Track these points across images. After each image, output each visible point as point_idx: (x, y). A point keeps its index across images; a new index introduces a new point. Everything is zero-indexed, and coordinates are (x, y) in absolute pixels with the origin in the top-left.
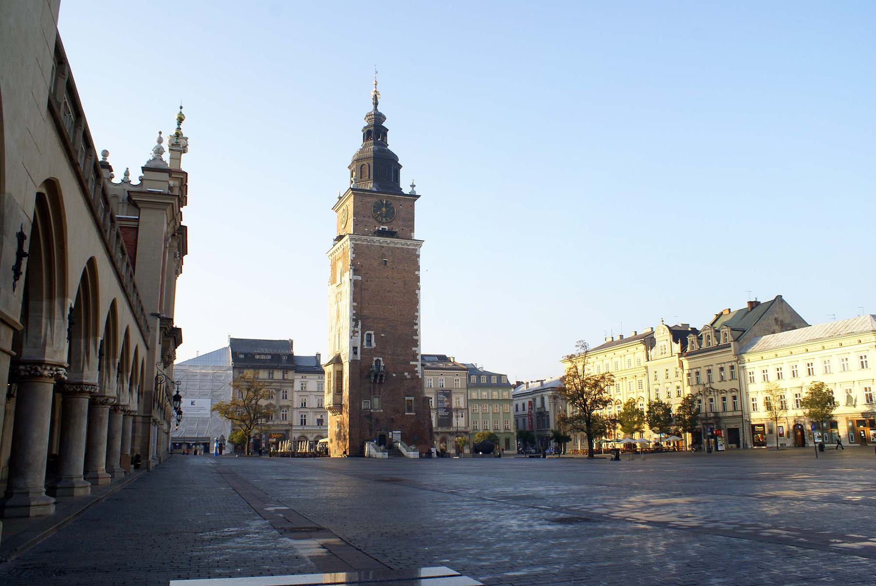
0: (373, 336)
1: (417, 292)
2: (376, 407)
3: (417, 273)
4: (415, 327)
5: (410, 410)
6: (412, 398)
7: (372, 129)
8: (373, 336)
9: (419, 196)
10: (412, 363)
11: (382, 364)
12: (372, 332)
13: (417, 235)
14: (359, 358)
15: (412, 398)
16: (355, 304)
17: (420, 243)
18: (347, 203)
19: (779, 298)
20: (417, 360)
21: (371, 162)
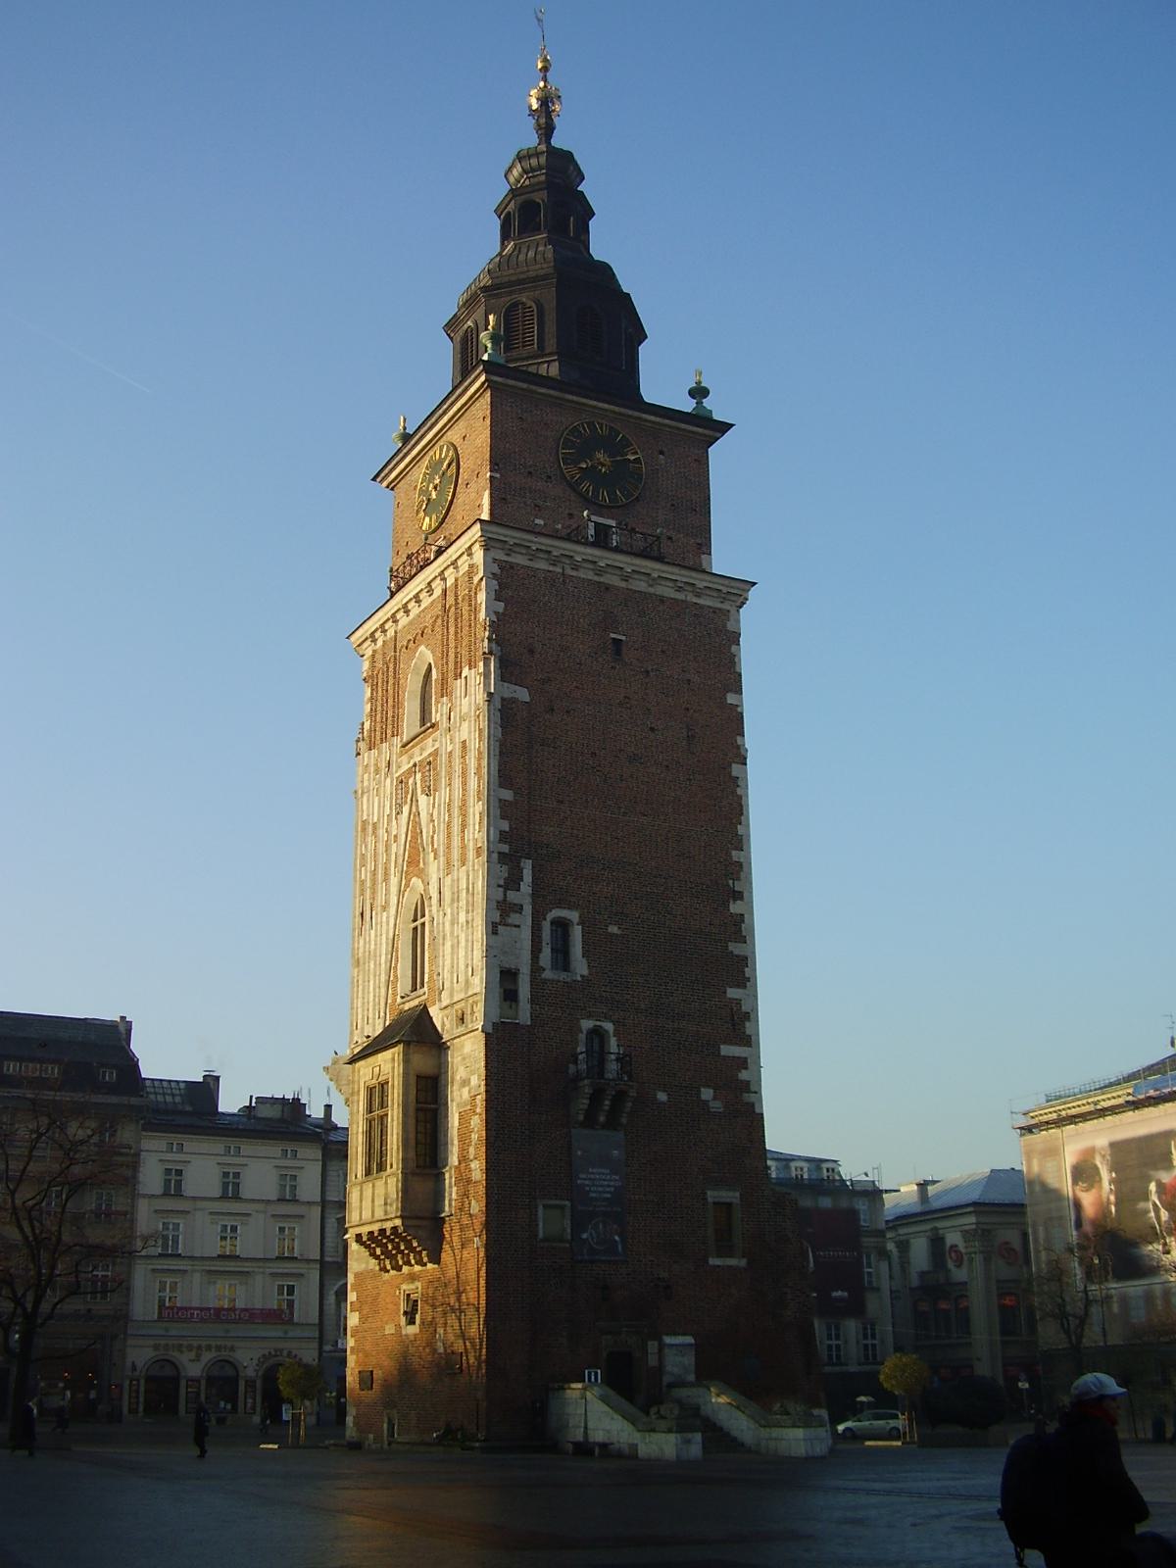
0: (577, 933)
3: (731, 699)
4: (735, 908)
6: (732, 1196)
7: (541, 197)
8: (577, 933)
9: (724, 427)
10: (727, 1050)
11: (613, 1044)
12: (574, 916)
13: (723, 560)
14: (524, 1014)
15: (732, 1196)
16: (507, 795)
17: (737, 591)
18: (454, 435)
21: (549, 296)
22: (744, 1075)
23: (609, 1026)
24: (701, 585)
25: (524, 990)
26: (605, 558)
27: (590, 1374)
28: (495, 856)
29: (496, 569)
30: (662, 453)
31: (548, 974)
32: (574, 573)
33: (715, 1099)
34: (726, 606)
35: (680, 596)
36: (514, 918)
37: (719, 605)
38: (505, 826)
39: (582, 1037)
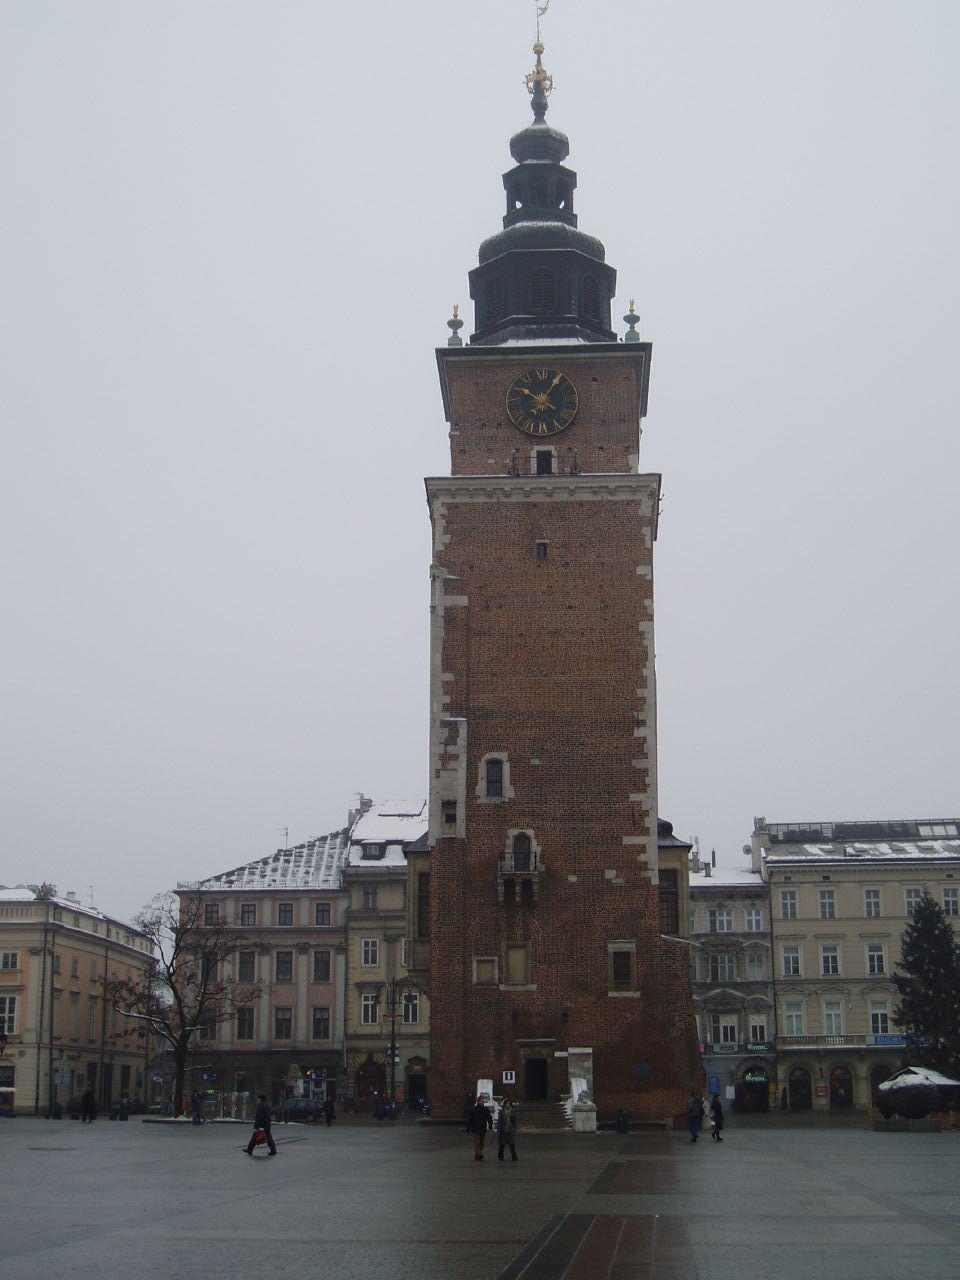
0: (506, 768)
1: (642, 626)
2: (518, 974)
4: (639, 733)
5: (622, 977)
6: (630, 946)
10: (627, 840)
12: (503, 756)
14: (460, 830)
16: (449, 677)
19: (650, 345)
20: (645, 832)
22: (643, 858)
23: (530, 832)
24: (612, 486)
25: (461, 812)
26: (528, 484)
27: (506, 1074)
28: (438, 723)
29: (444, 511)
30: (595, 380)
31: (483, 800)
32: (507, 500)
33: (617, 876)
34: (638, 496)
35: (597, 498)
36: (452, 764)
37: (631, 497)
38: (447, 699)
39: (510, 842)
